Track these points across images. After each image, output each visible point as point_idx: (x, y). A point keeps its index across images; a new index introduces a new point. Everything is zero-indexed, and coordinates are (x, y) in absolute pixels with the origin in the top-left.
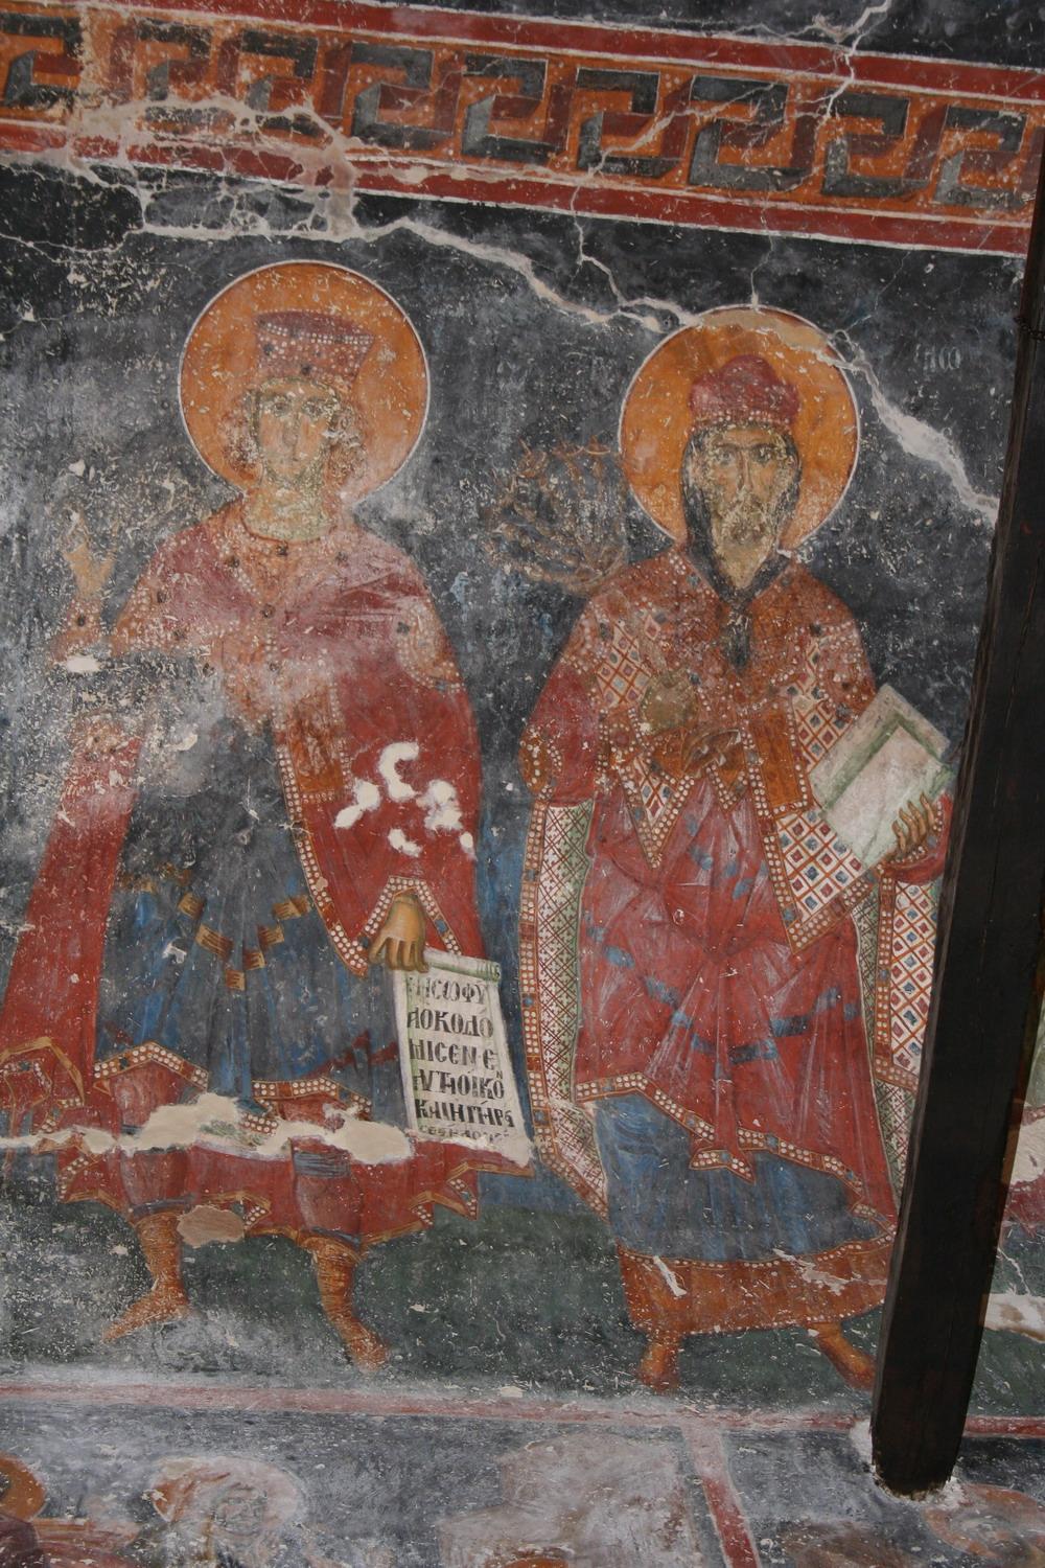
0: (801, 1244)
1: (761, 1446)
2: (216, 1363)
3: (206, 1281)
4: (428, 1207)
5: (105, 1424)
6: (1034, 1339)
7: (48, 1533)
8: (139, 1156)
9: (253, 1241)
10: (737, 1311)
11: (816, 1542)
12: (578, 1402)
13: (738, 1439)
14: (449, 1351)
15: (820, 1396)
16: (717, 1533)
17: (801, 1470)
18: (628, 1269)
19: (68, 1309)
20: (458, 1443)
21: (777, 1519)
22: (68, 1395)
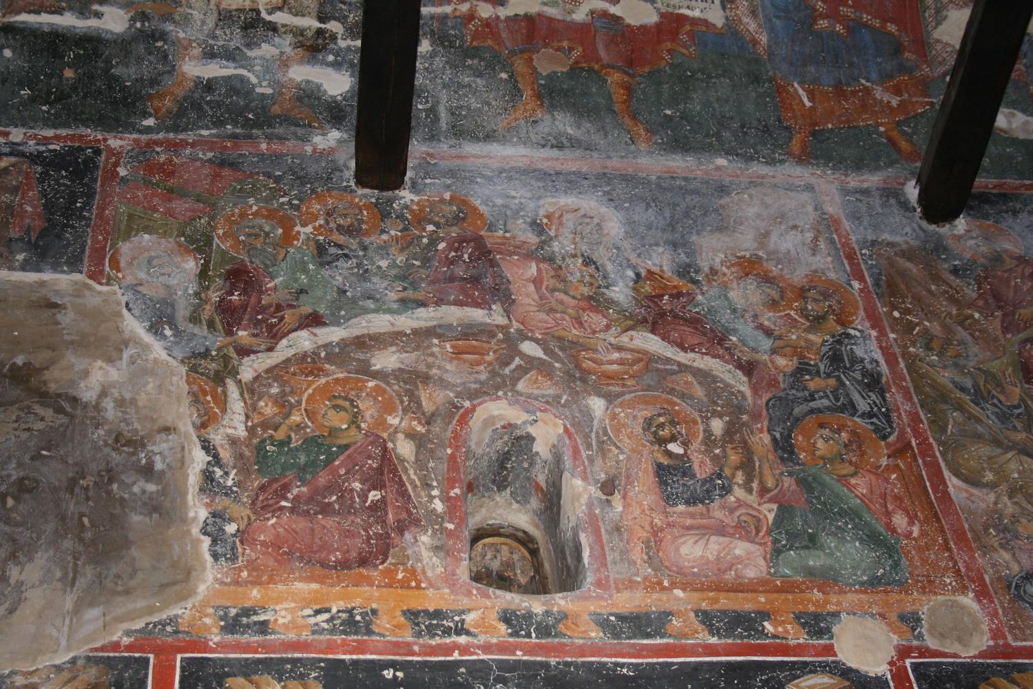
0: (874, 76)
1: (858, 196)
2: (562, 143)
3: (552, 95)
4: (668, 51)
5: (510, 178)
6: (1002, 134)
7: (492, 241)
8: (508, 19)
9: (575, 70)
10: (840, 116)
11: (891, 252)
12: (758, 169)
13: (845, 191)
14: (686, 137)
15: (887, 166)
16: (839, 246)
17: (880, 210)
18: (780, 90)
19: (479, 109)
20: (696, 192)
21: (869, 238)
22: (489, 161)
